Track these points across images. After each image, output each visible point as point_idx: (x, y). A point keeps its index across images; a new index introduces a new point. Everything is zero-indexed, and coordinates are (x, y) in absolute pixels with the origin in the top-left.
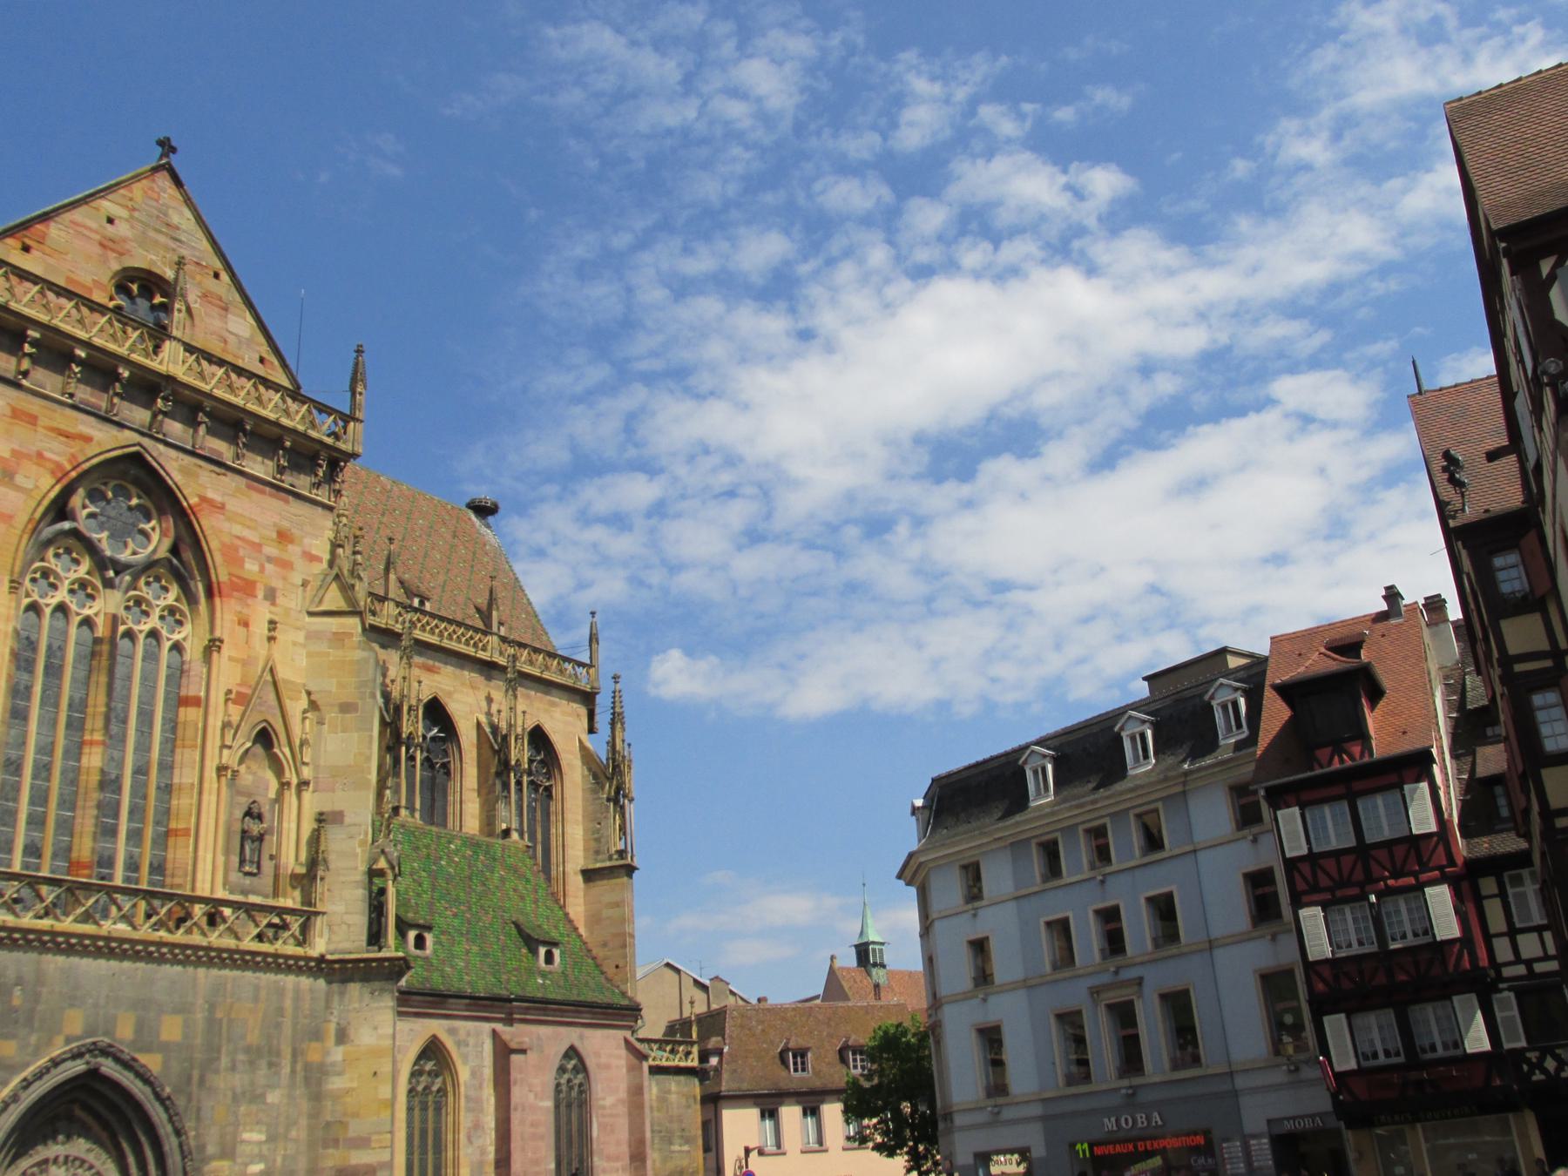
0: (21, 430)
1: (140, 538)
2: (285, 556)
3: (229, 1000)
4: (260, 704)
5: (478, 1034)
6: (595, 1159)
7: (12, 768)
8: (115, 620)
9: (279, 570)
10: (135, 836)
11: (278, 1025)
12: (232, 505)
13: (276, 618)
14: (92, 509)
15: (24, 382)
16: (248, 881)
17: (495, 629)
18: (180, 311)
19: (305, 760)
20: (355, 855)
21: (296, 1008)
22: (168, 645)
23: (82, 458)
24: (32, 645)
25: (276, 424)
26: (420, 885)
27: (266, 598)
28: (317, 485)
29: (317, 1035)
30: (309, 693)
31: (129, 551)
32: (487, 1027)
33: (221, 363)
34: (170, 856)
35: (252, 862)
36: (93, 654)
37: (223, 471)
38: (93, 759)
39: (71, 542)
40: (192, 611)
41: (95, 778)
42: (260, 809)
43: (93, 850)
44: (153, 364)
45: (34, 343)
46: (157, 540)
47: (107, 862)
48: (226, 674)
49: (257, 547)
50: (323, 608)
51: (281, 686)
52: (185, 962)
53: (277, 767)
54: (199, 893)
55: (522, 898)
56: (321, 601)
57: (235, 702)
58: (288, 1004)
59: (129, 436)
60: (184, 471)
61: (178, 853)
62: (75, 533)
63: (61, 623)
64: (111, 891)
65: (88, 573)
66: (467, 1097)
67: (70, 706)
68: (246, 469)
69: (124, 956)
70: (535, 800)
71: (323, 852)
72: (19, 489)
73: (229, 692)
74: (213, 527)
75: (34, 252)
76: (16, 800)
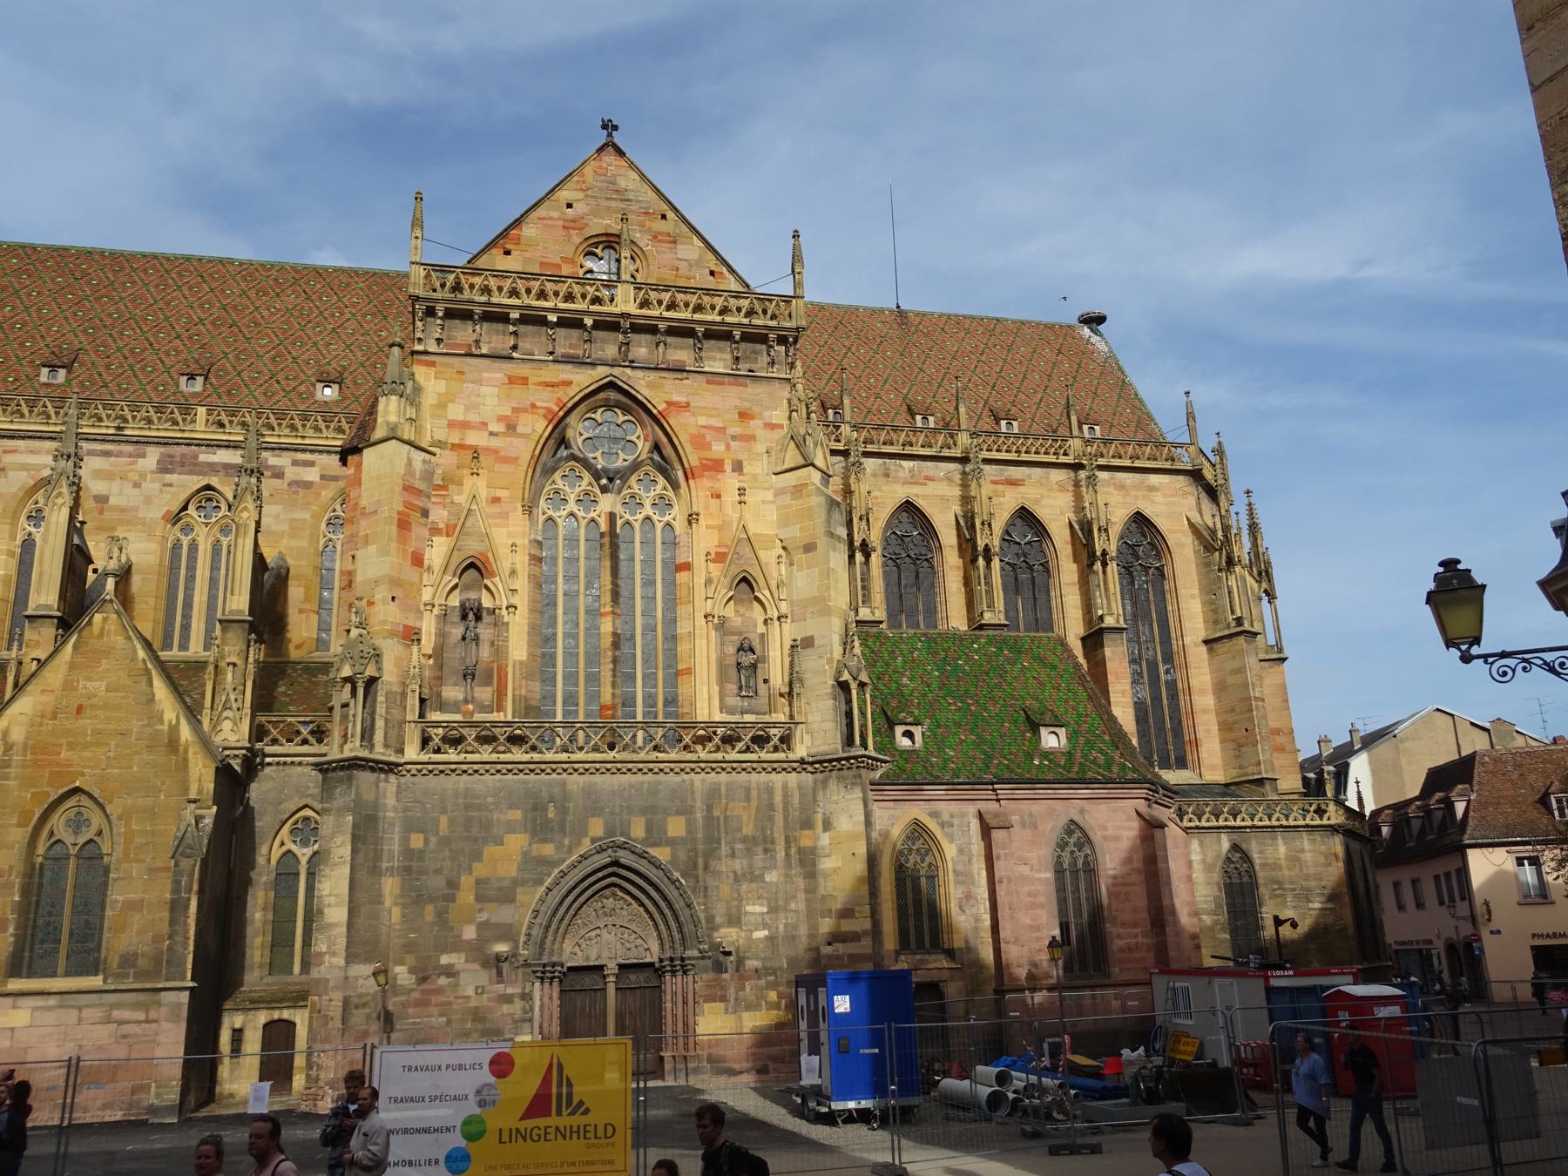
0: (518, 391)
2: (749, 432)
3: (724, 801)
5: (963, 815)
6: (1107, 925)
8: (612, 517)
9: (742, 444)
10: (649, 678)
11: (771, 819)
13: (742, 484)
15: (515, 355)
17: (1076, 432)
21: (786, 804)
22: (659, 526)
25: (723, 323)
26: (928, 686)
27: (733, 470)
29: (807, 824)
31: (620, 460)
32: (972, 809)
33: (667, 288)
34: (680, 691)
35: (748, 687)
36: (602, 545)
37: (685, 374)
38: (607, 626)
39: (573, 463)
40: (676, 495)
43: (613, 695)
46: (643, 447)
47: (629, 702)
48: (703, 541)
49: (722, 430)
50: (786, 466)
55: (1042, 685)
57: (714, 561)
58: (778, 798)
60: (650, 386)
61: (683, 690)
62: (574, 457)
66: (954, 871)
68: (706, 369)
70: (1147, 582)
73: (708, 554)
76: (554, 666)
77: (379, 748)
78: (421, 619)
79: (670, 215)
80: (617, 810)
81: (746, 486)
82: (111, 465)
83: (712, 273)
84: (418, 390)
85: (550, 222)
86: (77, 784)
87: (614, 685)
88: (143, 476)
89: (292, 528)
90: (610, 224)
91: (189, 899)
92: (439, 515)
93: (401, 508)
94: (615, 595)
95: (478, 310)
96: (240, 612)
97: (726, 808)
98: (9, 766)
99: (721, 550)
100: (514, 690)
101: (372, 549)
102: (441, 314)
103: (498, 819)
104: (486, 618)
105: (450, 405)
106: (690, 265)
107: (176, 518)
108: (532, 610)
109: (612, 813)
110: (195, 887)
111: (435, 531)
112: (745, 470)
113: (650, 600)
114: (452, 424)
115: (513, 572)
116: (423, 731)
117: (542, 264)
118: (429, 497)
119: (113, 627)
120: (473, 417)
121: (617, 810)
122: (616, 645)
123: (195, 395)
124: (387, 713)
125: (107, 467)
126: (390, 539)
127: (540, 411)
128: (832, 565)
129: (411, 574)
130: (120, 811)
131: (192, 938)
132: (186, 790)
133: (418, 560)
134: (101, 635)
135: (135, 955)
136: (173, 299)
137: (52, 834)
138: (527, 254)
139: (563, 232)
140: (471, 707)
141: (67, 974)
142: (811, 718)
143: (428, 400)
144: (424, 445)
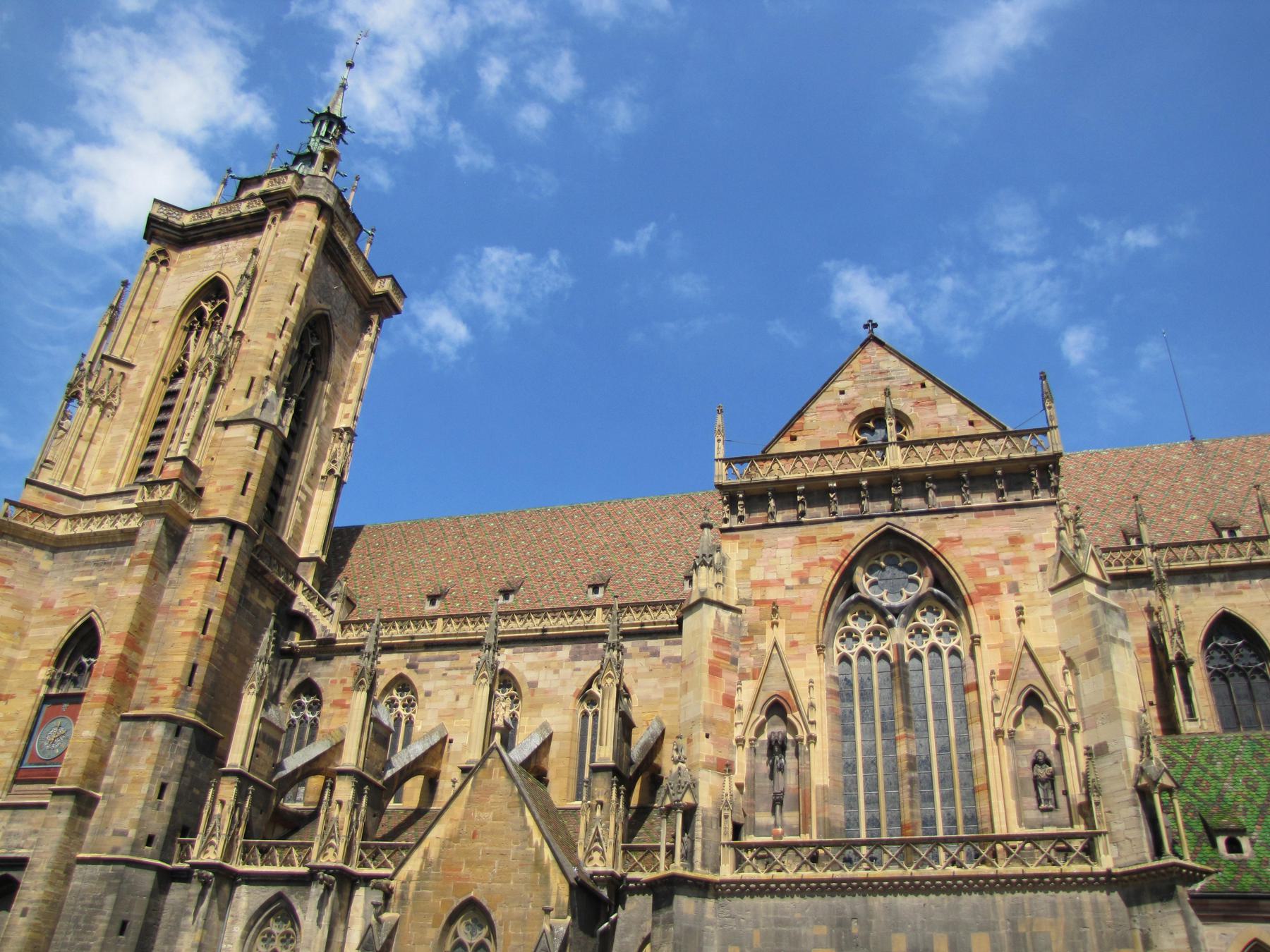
1: (912, 585)
2: (1021, 554)
4: (1023, 674)
7: (850, 769)
8: (899, 649)
9: (1016, 566)
10: (948, 798)
11: (1082, 936)
12: (967, 535)
13: (1019, 604)
14: (872, 578)
15: (803, 519)
16: (1046, 816)
18: (891, 424)
19: (1070, 707)
20: (1121, 777)
21: (1098, 920)
23: (849, 550)
24: (849, 683)
25: (984, 463)
27: (1010, 592)
28: (1036, 491)
30: (1064, 653)
31: (904, 596)
35: (1047, 800)
36: (892, 675)
41: (903, 764)
42: (1045, 755)
43: (912, 815)
44: (882, 467)
45: (802, 493)
46: (924, 583)
47: (929, 821)
49: (994, 557)
51: (1036, 654)
52: (980, 890)
53: (1049, 719)
54: (997, 833)
56: (1056, 577)
57: (1000, 678)
58: (1088, 916)
59: (879, 522)
60: (925, 527)
61: (982, 806)
62: (861, 600)
63: (865, 662)
64: (938, 842)
65: (878, 622)
67: (883, 716)
68: (974, 505)
69: (927, 891)
71: (1093, 781)
72: (813, 586)
73: (993, 672)
74: (955, 557)
76: (856, 790)
77: (698, 867)
78: (734, 753)
79: (929, 383)
80: (919, 927)
81: (1023, 605)
83: (971, 423)
84: (724, 561)
85: (826, 408)
86: (472, 894)
87: (912, 804)
89: (666, 696)
90: (878, 400)
92: (747, 662)
93: (712, 658)
94: (908, 720)
97: (1032, 924)
99: (1005, 667)
100: (817, 813)
102: (741, 496)
103: (805, 934)
104: (790, 750)
105: (752, 569)
106: (950, 420)
108: (832, 740)
109: (914, 930)
111: (743, 676)
112: (1021, 590)
113: (942, 720)
114: (755, 585)
115: (812, 706)
117: (822, 443)
118: (737, 648)
119: (498, 769)
120: (771, 576)
121: (919, 927)
122: (911, 767)
123: (597, 600)
124: (704, 835)
127: (828, 563)
128: (1116, 668)
129: (723, 715)
130: (500, 918)
132: (548, 902)
133: (729, 701)
134: (490, 776)
137: (456, 935)
138: (809, 437)
139: (837, 414)
140: (780, 830)
142: (1115, 827)
143: (733, 567)
144: (732, 604)
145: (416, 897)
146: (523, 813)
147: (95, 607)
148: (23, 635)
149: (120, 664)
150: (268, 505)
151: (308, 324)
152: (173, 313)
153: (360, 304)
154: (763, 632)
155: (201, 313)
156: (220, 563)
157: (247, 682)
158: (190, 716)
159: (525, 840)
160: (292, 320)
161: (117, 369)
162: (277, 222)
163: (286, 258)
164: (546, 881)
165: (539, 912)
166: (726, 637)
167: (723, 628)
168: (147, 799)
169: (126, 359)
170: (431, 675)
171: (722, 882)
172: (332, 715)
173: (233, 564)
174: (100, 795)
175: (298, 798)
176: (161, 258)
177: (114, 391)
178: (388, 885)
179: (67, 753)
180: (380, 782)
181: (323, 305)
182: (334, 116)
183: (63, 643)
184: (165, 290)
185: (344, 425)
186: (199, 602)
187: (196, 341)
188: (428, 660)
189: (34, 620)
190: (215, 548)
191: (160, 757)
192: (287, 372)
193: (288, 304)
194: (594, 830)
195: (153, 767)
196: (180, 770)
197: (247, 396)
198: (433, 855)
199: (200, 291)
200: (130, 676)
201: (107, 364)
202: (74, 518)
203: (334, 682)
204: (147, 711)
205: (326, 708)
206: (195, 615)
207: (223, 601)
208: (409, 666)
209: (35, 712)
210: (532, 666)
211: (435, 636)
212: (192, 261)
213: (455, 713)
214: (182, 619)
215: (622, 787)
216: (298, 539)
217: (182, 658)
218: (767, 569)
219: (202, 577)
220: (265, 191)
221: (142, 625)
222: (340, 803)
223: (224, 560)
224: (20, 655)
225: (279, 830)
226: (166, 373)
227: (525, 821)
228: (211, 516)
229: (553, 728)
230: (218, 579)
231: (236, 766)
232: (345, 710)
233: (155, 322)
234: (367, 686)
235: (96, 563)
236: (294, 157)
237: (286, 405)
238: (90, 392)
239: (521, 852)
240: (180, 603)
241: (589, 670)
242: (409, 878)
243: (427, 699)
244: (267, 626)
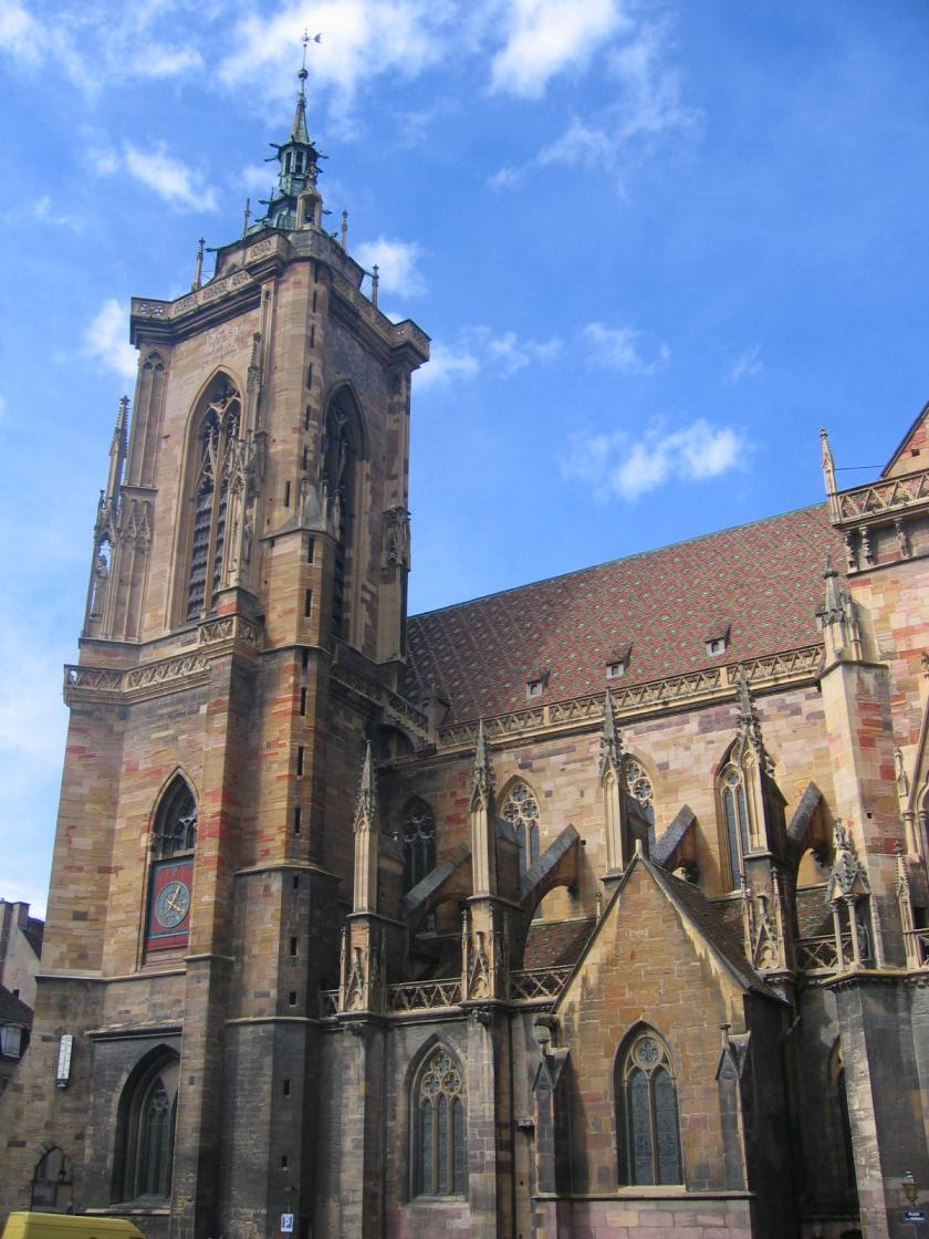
75: (921, 452)
78: (903, 829)
82: (665, 735)
86: (641, 1019)
88: (690, 739)
91: (736, 1116)
93: (861, 727)
95: (897, 518)
96: (761, 848)
98: (591, 1009)
101: (843, 771)
105: (891, 616)
107: (723, 770)
110: (739, 1105)
111: (903, 741)
114: (897, 634)
116: (922, 942)
120: (915, 621)
125: (662, 738)
126: (856, 760)
130: (676, 1040)
131: (743, 1152)
132: (724, 1018)
133: (888, 772)
135: (707, 1166)
136: (695, 577)
137: (631, 1063)
141: (659, 1183)
145: (583, 1028)
146: (680, 925)
147: (180, 763)
148: (115, 803)
149: (222, 822)
150: (334, 617)
151: (333, 403)
152: (183, 423)
153: (381, 360)
154: (916, 688)
155: (213, 414)
156: (300, 695)
157: (356, 819)
158: (305, 864)
159: (688, 955)
160: (315, 406)
161: (140, 499)
162: (272, 296)
163: (292, 336)
164: (718, 995)
165: (715, 1028)
166: (874, 700)
167: (869, 690)
168: (281, 956)
169: (149, 486)
170: (548, 772)
171: (910, 976)
172: (449, 832)
173: (314, 694)
174: (233, 958)
175: (429, 927)
176: (155, 363)
177: (144, 524)
178: (551, 1020)
179: (191, 922)
180: (517, 904)
181: (341, 376)
182: (301, 145)
183: (156, 806)
184: (170, 398)
185: (394, 506)
186: (288, 743)
187: (215, 449)
188: (541, 757)
189: (122, 785)
190: (291, 680)
191: (284, 911)
192: (321, 464)
193: (306, 390)
194: (759, 929)
195: (278, 923)
196: (307, 922)
197: (287, 505)
198: (593, 980)
199: (205, 393)
200: (235, 832)
201: (130, 497)
202: (138, 673)
203: (445, 795)
204: (260, 866)
205: (441, 827)
206: (287, 756)
207: (312, 737)
208: (522, 767)
209: (147, 881)
210: (658, 745)
211: (545, 728)
212: (189, 358)
213: (584, 811)
214: (275, 762)
215: (784, 877)
216: (371, 643)
217: (284, 804)
218: (908, 615)
219: (284, 713)
220: (250, 263)
221: (235, 776)
222: (481, 934)
223: (304, 690)
224: (119, 824)
225: (419, 968)
226: (192, 494)
227: (684, 931)
228: (278, 646)
229: (695, 812)
230: (303, 714)
231: (364, 910)
232: (461, 825)
233: (167, 437)
234: (484, 803)
235: (170, 716)
236: (268, 206)
237: (330, 504)
238: (119, 530)
239: (685, 968)
240: (269, 745)
241: (723, 741)
242: (571, 1007)
243: (549, 799)
244: (365, 756)
